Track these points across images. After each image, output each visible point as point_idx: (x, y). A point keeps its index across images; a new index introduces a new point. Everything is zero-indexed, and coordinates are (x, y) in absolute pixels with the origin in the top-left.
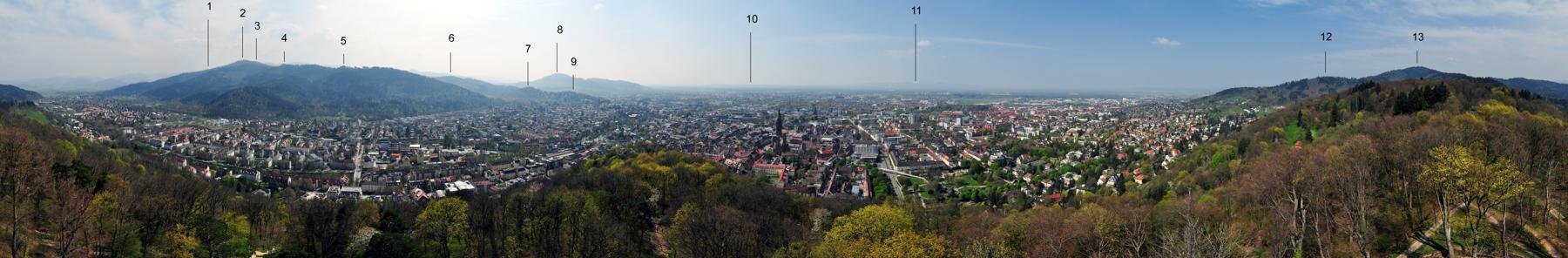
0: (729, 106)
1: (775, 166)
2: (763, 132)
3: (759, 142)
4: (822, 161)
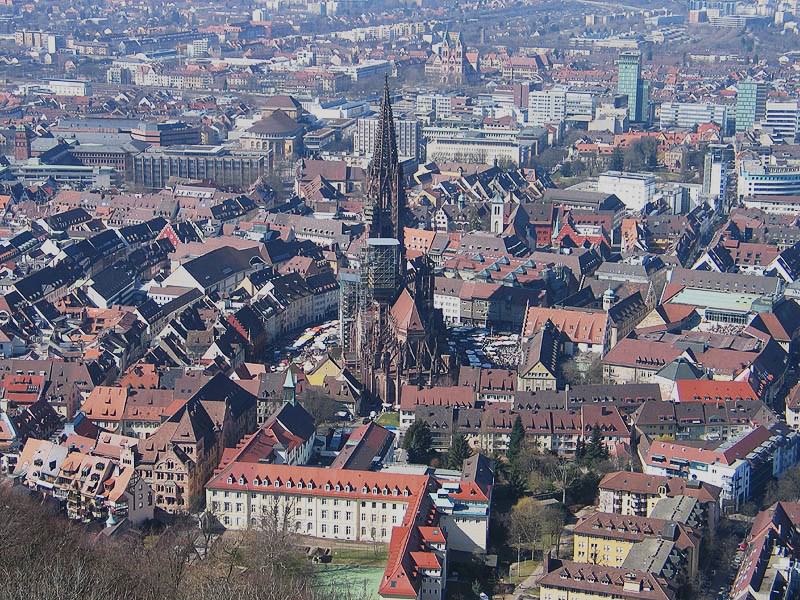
0: (32, 69)
1: (358, 477)
2: (278, 247)
3: (248, 316)
4: (679, 452)
